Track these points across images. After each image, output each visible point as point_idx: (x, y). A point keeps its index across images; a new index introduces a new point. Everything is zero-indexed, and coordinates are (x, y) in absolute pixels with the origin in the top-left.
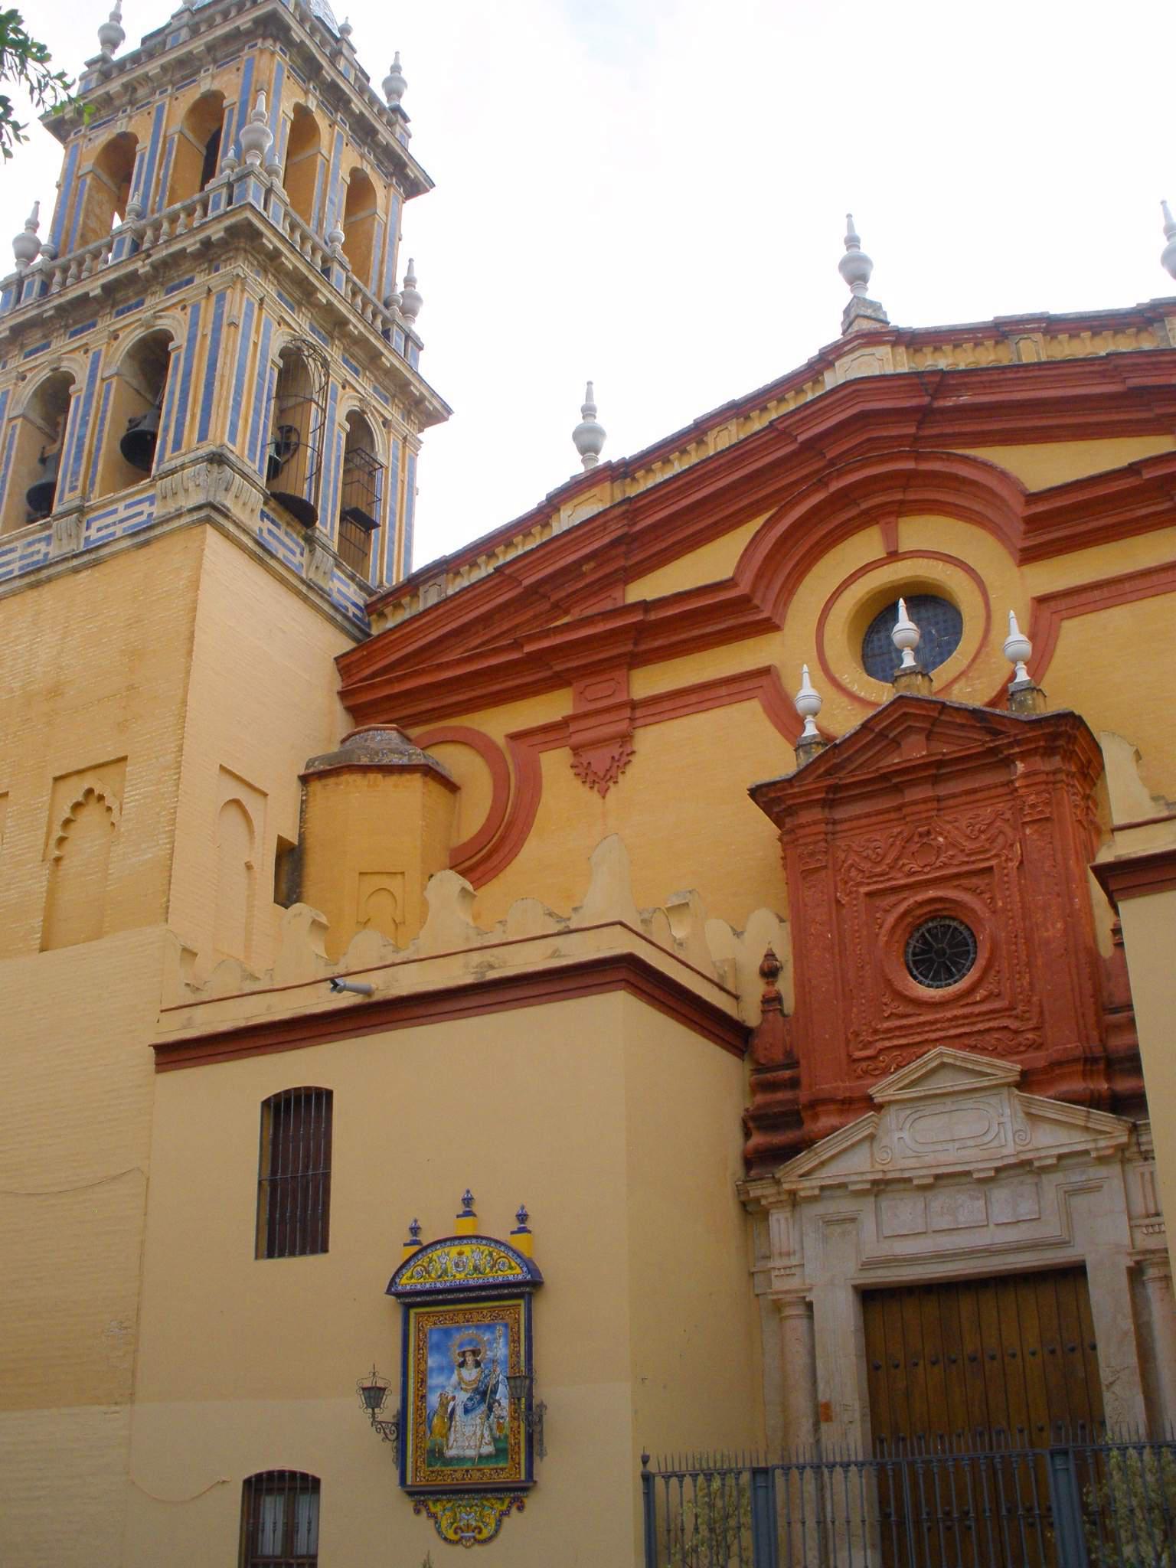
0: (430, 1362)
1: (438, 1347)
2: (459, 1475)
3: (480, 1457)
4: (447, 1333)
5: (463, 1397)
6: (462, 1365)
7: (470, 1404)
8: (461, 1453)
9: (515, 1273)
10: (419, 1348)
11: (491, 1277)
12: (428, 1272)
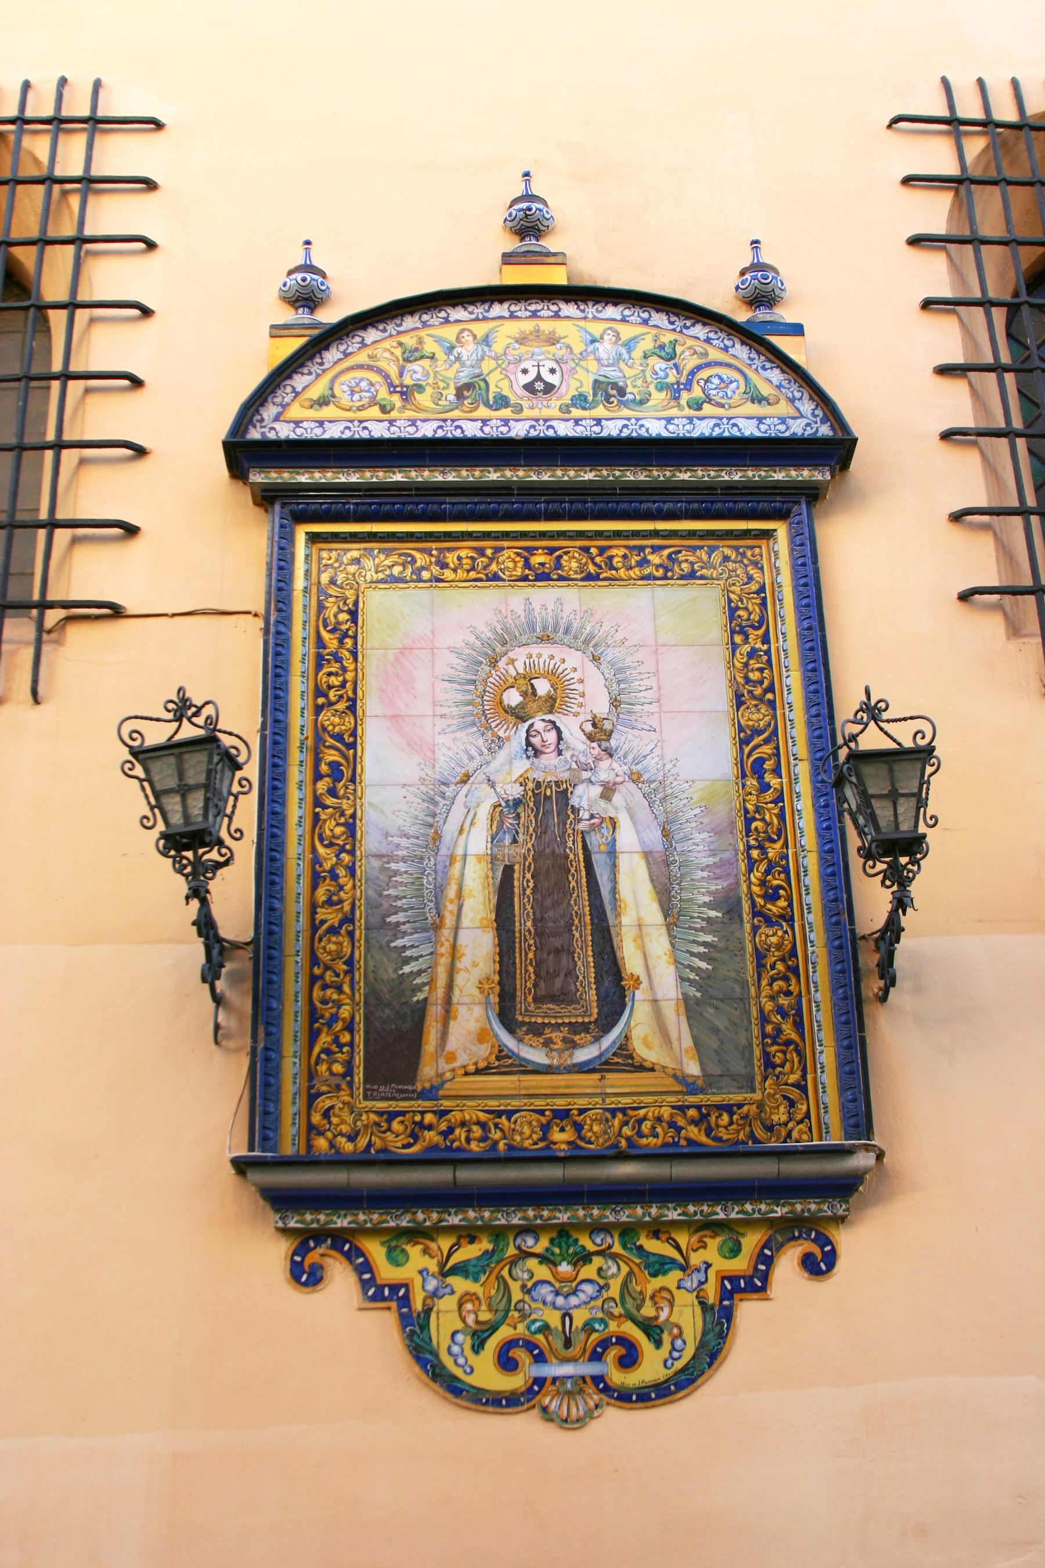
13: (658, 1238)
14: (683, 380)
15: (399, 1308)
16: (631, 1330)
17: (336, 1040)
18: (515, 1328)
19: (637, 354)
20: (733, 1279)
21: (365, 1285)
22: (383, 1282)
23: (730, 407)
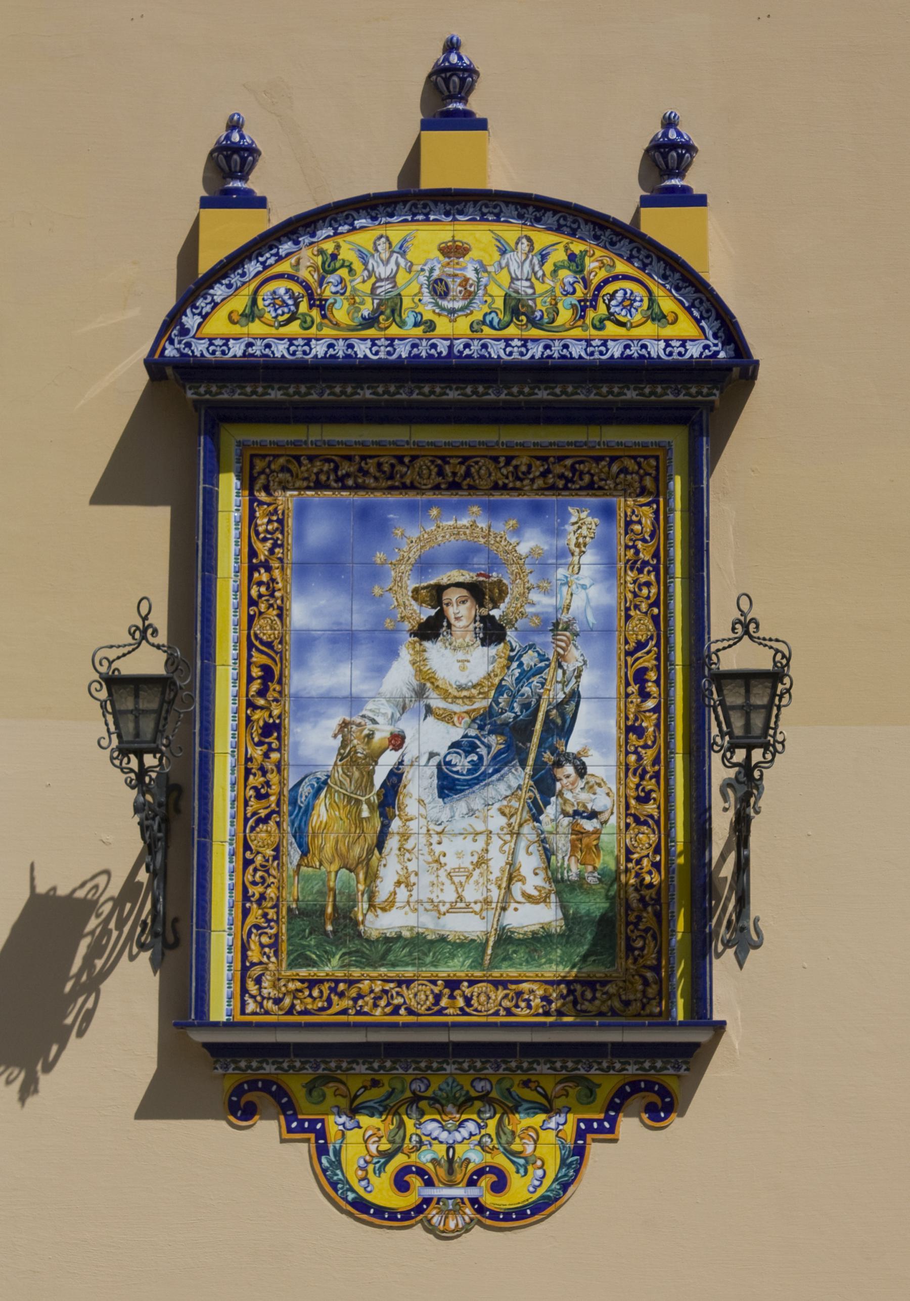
0: (301, 613)
1: (329, 566)
2: (418, 997)
3: (506, 939)
4: (371, 523)
5: (431, 738)
6: (430, 630)
7: (462, 763)
8: (427, 923)
9: (681, 334)
10: (253, 564)
11: (575, 341)
12: (321, 305)
13: (529, 1087)
14: (589, 297)
15: (317, 1140)
16: (501, 1161)
17: (265, 915)
18: (409, 1157)
19: (548, 267)
20: (588, 1122)
23: (632, 327)
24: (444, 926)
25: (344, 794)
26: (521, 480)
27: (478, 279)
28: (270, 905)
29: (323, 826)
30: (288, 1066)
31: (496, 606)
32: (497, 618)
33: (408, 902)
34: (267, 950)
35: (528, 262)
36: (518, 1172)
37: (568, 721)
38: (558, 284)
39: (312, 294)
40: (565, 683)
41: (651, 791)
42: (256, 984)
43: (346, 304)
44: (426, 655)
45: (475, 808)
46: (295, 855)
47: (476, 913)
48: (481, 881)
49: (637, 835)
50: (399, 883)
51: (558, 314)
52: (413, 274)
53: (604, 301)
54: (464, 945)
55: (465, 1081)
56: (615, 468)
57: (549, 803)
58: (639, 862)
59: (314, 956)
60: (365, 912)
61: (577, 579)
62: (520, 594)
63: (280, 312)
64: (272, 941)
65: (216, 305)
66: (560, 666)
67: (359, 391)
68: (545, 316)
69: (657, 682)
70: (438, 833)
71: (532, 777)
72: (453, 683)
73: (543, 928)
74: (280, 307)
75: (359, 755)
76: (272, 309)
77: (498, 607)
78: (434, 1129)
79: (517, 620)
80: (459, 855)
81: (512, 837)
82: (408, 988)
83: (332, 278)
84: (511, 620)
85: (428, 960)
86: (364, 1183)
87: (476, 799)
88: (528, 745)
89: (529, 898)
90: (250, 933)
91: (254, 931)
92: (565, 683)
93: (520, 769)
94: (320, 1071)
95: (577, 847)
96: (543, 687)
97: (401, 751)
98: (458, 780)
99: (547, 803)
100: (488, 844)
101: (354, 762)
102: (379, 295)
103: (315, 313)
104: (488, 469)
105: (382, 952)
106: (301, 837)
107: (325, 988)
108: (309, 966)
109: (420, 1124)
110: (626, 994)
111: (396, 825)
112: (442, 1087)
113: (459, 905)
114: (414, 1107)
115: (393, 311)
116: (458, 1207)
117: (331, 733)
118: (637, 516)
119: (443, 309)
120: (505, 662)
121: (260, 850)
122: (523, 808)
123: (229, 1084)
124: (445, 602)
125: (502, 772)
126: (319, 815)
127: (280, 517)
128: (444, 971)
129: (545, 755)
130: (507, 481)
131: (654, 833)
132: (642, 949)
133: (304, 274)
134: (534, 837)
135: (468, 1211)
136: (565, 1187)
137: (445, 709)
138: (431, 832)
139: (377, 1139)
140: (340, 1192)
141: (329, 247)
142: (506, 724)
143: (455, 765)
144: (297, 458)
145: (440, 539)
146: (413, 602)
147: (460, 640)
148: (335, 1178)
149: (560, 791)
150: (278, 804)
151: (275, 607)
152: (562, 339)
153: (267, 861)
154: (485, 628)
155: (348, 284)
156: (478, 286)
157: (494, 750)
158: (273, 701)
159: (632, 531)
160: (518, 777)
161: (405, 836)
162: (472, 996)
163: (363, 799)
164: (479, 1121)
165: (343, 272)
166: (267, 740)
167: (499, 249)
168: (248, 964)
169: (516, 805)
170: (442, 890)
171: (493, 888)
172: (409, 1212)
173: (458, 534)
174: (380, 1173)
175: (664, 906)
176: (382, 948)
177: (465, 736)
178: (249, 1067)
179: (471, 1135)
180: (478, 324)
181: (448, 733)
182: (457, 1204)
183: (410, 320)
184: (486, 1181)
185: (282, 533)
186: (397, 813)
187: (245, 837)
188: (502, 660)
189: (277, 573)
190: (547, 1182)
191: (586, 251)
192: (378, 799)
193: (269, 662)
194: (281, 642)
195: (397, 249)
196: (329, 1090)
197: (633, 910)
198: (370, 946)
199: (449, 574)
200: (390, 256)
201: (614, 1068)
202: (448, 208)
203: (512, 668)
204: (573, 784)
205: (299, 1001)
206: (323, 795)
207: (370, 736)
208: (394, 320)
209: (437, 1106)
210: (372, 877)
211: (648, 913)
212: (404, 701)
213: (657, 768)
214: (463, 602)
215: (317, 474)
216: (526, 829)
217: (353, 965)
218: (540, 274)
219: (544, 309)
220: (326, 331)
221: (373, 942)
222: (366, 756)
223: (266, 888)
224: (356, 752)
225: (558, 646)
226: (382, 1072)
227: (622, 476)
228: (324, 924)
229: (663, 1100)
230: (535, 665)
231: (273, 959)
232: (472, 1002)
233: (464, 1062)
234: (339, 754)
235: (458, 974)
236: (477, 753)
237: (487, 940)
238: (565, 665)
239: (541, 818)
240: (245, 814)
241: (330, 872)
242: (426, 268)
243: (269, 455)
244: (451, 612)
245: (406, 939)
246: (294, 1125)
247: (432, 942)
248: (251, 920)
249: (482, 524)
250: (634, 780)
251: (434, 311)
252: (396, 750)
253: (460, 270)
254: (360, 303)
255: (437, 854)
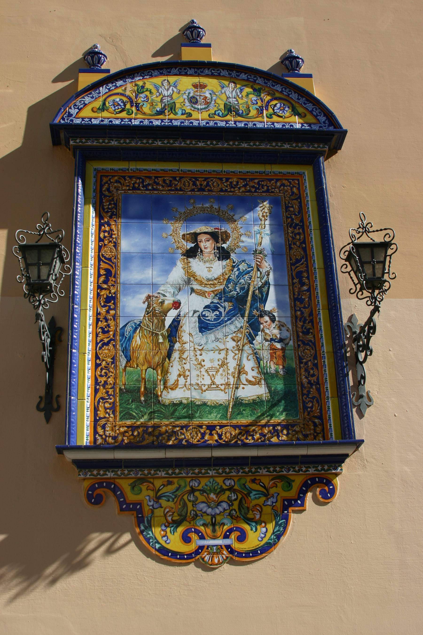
0: (125, 245)
3: (239, 404)
5: (194, 304)
6: (193, 253)
7: (211, 316)
8: (196, 396)
13: (255, 483)
17: (107, 392)
21: (121, 504)
22: (130, 502)
23: (285, 118)
24: (205, 397)
25: (149, 331)
26: (234, 188)
27: (211, 97)
28: (110, 387)
29: (138, 347)
30: (121, 473)
31: (225, 243)
32: (226, 248)
33: (185, 385)
34: (108, 411)
35: (234, 91)
36: (252, 530)
37: (265, 296)
38: (249, 100)
39: (132, 101)
40: (261, 278)
41: (310, 329)
42: (102, 429)
43: (149, 106)
44: (190, 265)
45: (219, 337)
46: (123, 361)
47: (222, 390)
48: (224, 373)
49: (304, 350)
50: (179, 375)
51: (250, 112)
52: (180, 95)
53: (271, 107)
54: (217, 407)
55: (220, 480)
56: (278, 184)
57: (258, 335)
58: (306, 363)
59: (134, 414)
60: (162, 390)
61: (264, 231)
62: (236, 237)
63: (117, 108)
64: (111, 406)
65: (85, 105)
66: (258, 270)
67: (155, 142)
68: (244, 112)
69: (308, 278)
70: (200, 350)
71: (248, 322)
72: (204, 277)
73: (258, 397)
74: (117, 106)
75: (157, 312)
76: (113, 107)
77: (226, 243)
78: (204, 507)
79: (235, 249)
80: (212, 361)
81: (239, 352)
82: (186, 430)
83: (142, 95)
84: (233, 249)
85: (197, 415)
86: (165, 538)
87: (219, 333)
88: (245, 307)
89: (250, 382)
90: (99, 402)
91: (101, 401)
92: (261, 278)
93: (241, 318)
94: (139, 476)
95: (274, 356)
96: (250, 280)
97: (179, 310)
98: (209, 324)
99: (256, 335)
100: (227, 355)
101: (154, 315)
102: (164, 102)
103: (134, 109)
104: (217, 183)
105: (172, 411)
106: (126, 352)
107: (141, 430)
108: (132, 419)
109: (196, 505)
110: (305, 431)
111: (177, 346)
112: (207, 484)
113: (212, 386)
114: (192, 495)
115: (171, 109)
116: (219, 551)
117: (142, 301)
118: (291, 204)
119: (195, 108)
120: (231, 268)
121: (105, 359)
122: (244, 337)
123: (86, 484)
124: (199, 240)
125: (232, 320)
126: (136, 341)
127: (115, 202)
128: (206, 421)
129: (254, 312)
130: (227, 188)
131: (313, 349)
132: (312, 407)
133: (128, 93)
134: (250, 352)
135: (224, 552)
136: (279, 537)
137: (201, 290)
138: (196, 349)
139: (171, 513)
140: (151, 544)
141: (140, 83)
142: (232, 297)
143: (208, 317)
144: (124, 177)
145: (195, 213)
146: (183, 241)
147: (207, 258)
148: (148, 536)
149: (263, 329)
150: (114, 336)
151: (113, 242)
152: (253, 122)
153: (109, 364)
154: (219, 253)
155: (149, 98)
156: (211, 100)
157: (227, 309)
158: (111, 286)
159: (289, 210)
160: (240, 322)
161: (182, 352)
162: (222, 433)
163: (159, 333)
164: (229, 502)
165: (148, 93)
166: (108, 304)
167: (221, 86)
168: (98, 418)
169: (241, 336)
170: (203, 379)
171: (231, 377)
172: (191, 554)
173: (204, 210)
174: (174, 533)
175: (321, 386)
176: (171, 409)
177: (212, 303)
178: (98, 474)
179: (225, 510)
180: (212, 114)
181: (203, 301)
182: (218, 549)
183: (180, 112)
184: (233, 536)
185: (116, 209)
186: (178, 340)
187: (96, 353)
188: (229, 267)
189: (113, 227)
190: (269, 535)
191: (261, 88)
192: (167, 333)
193: (109, 267)
194: (115, 258)
195: (173, 85)
196: (144, 487)
197: (305, 388)
198: (166, 408)
199: (200, 228)
200: (170, 87)
201: (302, 470)
202: (196, 70)
203: (234, 271)
204: (269, 326)
205: (126, 438)
206: (138, 331)
207: (162, 303)
208: (172, 112)
209: (205, 494)
210: (165, 372)
211: (313, 389)
212: (180, 286)
213: (311, 318)
214: (208, 241)
215: (134, 184)
216: (246, 347)
217: (156, 418)
218: (240, 96)
219: (243, 110)
220: (139, 116)
221: (167, 406)
222: (160, 312)
223: (108, 378)
224: (155, 310)
225: (257, 261)
226: (174, 475)
227: (282, 187)
228: (140, 397)
229: (329, 488)
230: (246, 269)
231: (112, 416)
232: (222, 437)
233: (219, 469)
234: (146, 311)
235: (214, 422)
236: (219, 311)
237: (229, 404)
238: (261, 270)
239: (254, 342)
240: (96, 341)
241: (142, 370)
242: (186, 92)
243: (110, 176)
244: (202, 245)
245: (184, 404)
246: (124, 506)
247: (198, 406)
248: (99, 395)
249: (216, 206)
250: (300, 324)
251: (191, 109)
252: (176, 309)
253: (203, 93)
254: (155, 105)
255: (200, 361)
